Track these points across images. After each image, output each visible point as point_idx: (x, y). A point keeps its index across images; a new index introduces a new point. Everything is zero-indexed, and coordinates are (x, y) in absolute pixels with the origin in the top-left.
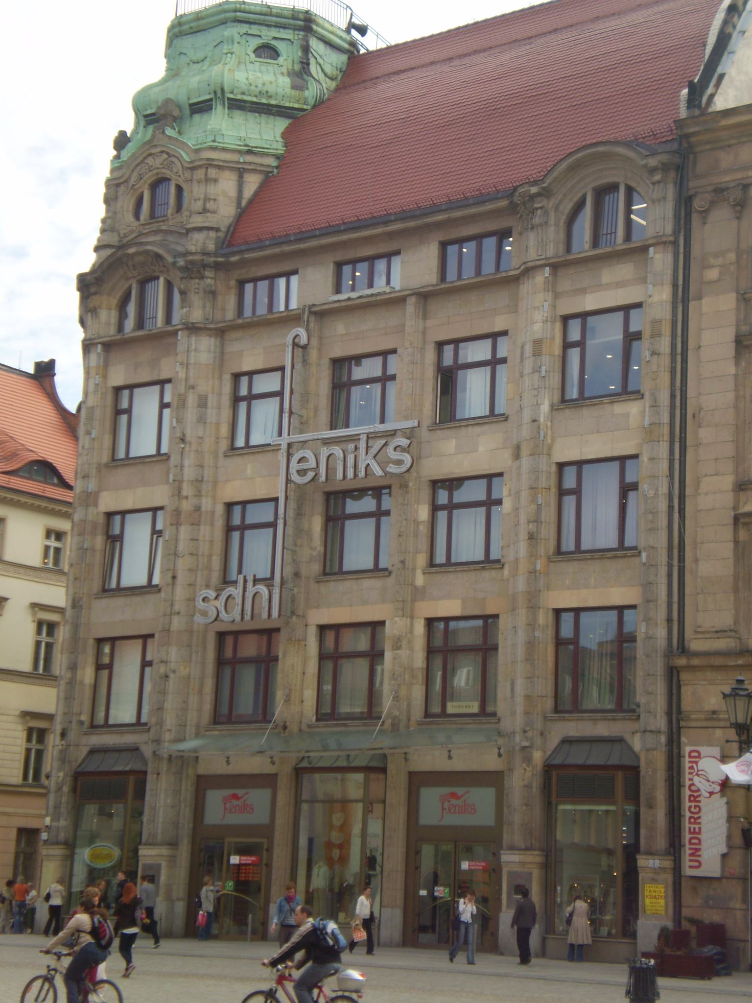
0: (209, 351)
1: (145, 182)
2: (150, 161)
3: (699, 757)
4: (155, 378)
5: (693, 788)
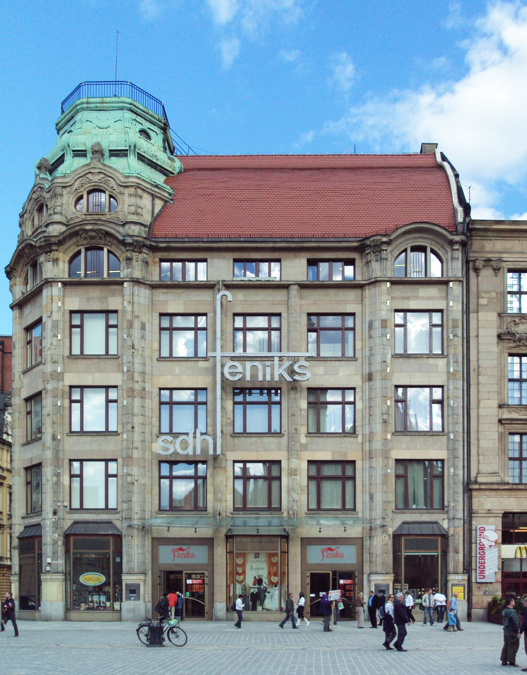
0: (145, 298)
1: (85, 189)
2: (89, 176)
3: (484, 530)
4: (104, 308)
5: (481, 544)
